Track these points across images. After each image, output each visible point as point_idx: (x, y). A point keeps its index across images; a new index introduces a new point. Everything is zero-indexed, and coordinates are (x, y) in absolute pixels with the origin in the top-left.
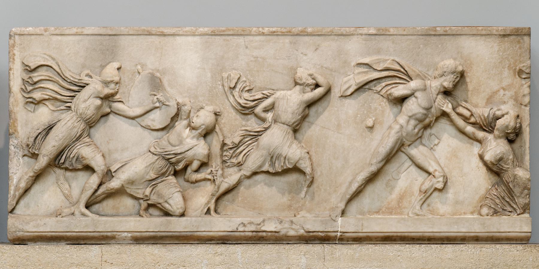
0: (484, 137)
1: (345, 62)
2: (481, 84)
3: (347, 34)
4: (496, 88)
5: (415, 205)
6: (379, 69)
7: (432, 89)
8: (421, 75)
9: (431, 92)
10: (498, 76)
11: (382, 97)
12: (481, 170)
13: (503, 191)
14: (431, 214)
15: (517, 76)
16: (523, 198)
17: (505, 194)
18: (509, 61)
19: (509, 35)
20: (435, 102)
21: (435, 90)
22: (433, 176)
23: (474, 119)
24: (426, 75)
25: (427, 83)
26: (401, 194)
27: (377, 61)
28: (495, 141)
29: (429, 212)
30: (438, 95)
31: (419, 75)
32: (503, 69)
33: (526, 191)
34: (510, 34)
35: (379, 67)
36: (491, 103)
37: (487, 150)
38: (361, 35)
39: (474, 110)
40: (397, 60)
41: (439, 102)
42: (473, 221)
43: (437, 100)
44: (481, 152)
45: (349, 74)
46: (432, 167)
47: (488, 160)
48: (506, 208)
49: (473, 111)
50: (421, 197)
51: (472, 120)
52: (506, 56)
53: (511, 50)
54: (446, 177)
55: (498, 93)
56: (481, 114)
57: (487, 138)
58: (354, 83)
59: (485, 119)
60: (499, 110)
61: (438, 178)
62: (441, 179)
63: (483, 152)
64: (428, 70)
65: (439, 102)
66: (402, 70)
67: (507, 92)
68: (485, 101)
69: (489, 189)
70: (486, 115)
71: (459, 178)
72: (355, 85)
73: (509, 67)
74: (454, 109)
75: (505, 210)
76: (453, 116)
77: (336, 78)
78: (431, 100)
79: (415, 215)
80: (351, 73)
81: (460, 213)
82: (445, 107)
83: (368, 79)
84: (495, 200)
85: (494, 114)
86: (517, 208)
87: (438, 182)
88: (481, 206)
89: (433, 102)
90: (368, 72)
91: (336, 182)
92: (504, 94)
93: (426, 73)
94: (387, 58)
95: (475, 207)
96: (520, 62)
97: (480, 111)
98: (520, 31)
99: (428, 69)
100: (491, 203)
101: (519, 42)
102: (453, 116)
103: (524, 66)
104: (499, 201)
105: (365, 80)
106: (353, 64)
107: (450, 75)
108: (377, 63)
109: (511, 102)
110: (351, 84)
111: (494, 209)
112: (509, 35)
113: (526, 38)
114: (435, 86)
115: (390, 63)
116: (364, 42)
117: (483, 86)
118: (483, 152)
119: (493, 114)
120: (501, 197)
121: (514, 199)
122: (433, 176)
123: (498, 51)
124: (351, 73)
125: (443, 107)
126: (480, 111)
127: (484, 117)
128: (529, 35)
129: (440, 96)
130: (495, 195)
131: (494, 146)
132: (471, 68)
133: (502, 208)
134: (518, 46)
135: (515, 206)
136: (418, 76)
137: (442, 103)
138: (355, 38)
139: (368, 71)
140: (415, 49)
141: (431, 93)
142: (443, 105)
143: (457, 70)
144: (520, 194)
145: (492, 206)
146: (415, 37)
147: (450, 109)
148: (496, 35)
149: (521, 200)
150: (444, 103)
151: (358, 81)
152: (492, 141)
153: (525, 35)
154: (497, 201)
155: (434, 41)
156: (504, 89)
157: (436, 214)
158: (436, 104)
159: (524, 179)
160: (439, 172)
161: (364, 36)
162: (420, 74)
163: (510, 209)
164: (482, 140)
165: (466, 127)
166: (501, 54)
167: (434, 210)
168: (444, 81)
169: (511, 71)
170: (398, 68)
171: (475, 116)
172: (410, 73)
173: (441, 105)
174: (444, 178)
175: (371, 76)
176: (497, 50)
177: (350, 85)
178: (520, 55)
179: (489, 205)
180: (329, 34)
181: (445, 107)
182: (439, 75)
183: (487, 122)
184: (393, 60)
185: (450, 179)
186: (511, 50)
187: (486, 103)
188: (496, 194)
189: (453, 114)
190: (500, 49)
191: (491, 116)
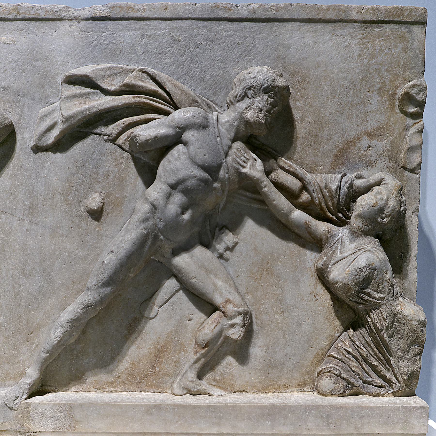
0: (329, 232)
1: (45, 75)
2: (323, 124)
3: (47, 17)
4: (353, 134)
5: (186, 372)
6: (112, 88)
7: (220, 126)
8: (200, 101)
9: (219, 131)
10: (359, 109)
11: (119, 150)
12: (319, 301)
13: (365, 344)
14: (219, 387)
15: (397, 110)
16: (409, 360)
17: (370, 350)
18: (381, 77)
19: (383, 22)
20: (226, 155)
21: (227, 130)
22: (223, 312)
23: (309, 196)
24: (211, 104)
25: (210, 115)
26: (159, 347)
27: (108, 72)
28: (351, 241)
29: (214, 383)
30: (234, 140)
31: (196, 102)
32: (368, 94)
33: (415, 348)
34: (386, 19)
35: (112, 85)
36: (343, 164)
37: (336, 260)
38: (77, 19)
39: (308, 177)
40: (149, 69)
41: (236, 155)
42: (306, 412)
43: (231, 152)
44: (322, 263)
45: (52, 100)
46: (221, 294)
47: (337, 282)
48: (371, 379)
49: (307, 180)
50: (198, 355)
51: (305, 197)
52: (375, 67)
53: (385, 55)
54: (248, 317)
55: (357, 143)
56: (322, 185)
57: (334, 235)
58: (61, 117)
59: (331, 196)
60: (359, 177)
61: (232, 317)
62: (239, 320)
63: (326, 265)
64: (214, 94)
65: (236, 155)
66: (160, 91)
67: (375, 142)
68: (331, 159)
69: (335, 339)
70: (334, 187)
71: (276, 315)
72: (64, 122)
73: (380, 89)
74: (268, 173)
75: (369, 383)
76: (265, 186)
77: (26, 110)
78: (219, 150)
79: (186, 391)
80: (58, 99)
81: (276, 386)
82: (248, 166)
83: (88, 109)
84: (349, 361)
85: (351, 185)
86: (395, 381)
87: (233, 326)
88: (319, 374)
89: (223, 155)
90: (91, 96)
91: (27, 322)
92: (369, 147)
93: (211, 99)
94: (130, 67)
95: (307, 373)
96: (405, 79)
97: (322, 180)
98: (406, 14)
99: (215, 91)
100: (341, 368)
101: (402, 37)
102: (265, 186)
103: (414, 86)
104: (357, 365)
105: (84, 111)
106: (60, 79)
107: (262, 94)
108: (110, 76)
109: (384, 162)
110: (55, 120)
111: (348, 382)
112: (383, 22)
113: (416, 29)
114: (228, 122)
115: (135, 77)
116: (83, 34)
117: (326, 129)
118: (326, 265)
119: (347, 185)
120: (362, 355)
121: (390, 365)
122: (223, 312)
123: (359, 55)
124: (58, 99)
125: (244, 167)
126: (322, 180)
127: (330, 191)
128: (423, 23)
129: (238, 145)
130: (349, 353)
131: (350, 252)
132: (303, 91)
133: (362, 379)
134: (400, 46)
135: (389, 376)
136: (194, 103)
137: (242, 158)
138: (64, 27)
139: (89, 93)
140: (189, 49)
141: (220, 136)
142: (245, 162)
143: (276, 83)
144: (403, 353)
145: (343, 375)
146: (189, 22)
147: (259, 171)
148: (356, 22)
149: (403, 364)
150: (248, 159)
151: (66, 113)
152: (346, 240)
153: (414, 23)
154: (354, 364)
155: (228, 31)
156: (370, 136)
157: (229, 389)
158: (229, 159)
159: (415, 323)
160: (235, 306)
161: (83, 23)
162: (197, 99)
163: (379, 381)
164: (324, 239)
165: (291, 211)
166: (366, 61)
167: (224, 379)
168: (246, 108)
169: (386, 99)
170: (153, 87)
171: (310, 188)
172: (177, 96)
173: (241, 162)
174: (244, 319)
175: (96, 103)
176: (356, 54)
177: (53, 122)
178: (405, 65)
179: (337, 373)
180: (11, 17)
181: (248, 166)
182: (236, 97)
183: (336, 201)
184: (142, 71)
185: (256, 318)
186: (385, 55)
187: (332, 164)
188: (350, 350)
189: (265, 183)
190: (365, 51)
191: (344, 189)
